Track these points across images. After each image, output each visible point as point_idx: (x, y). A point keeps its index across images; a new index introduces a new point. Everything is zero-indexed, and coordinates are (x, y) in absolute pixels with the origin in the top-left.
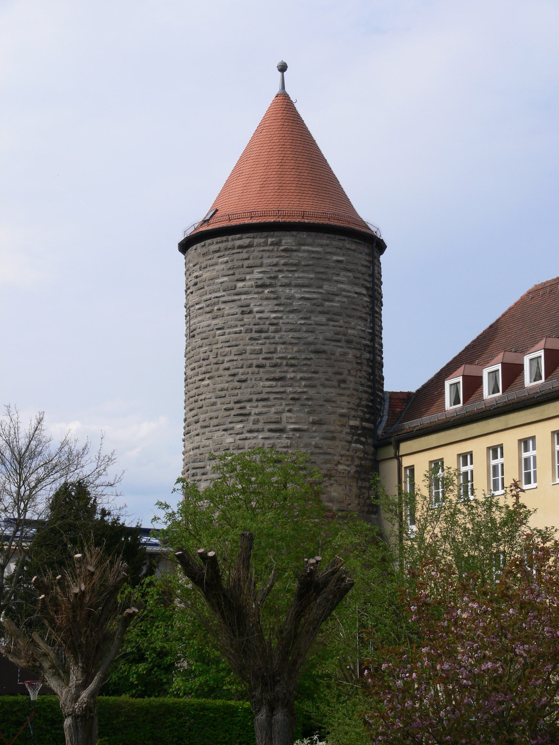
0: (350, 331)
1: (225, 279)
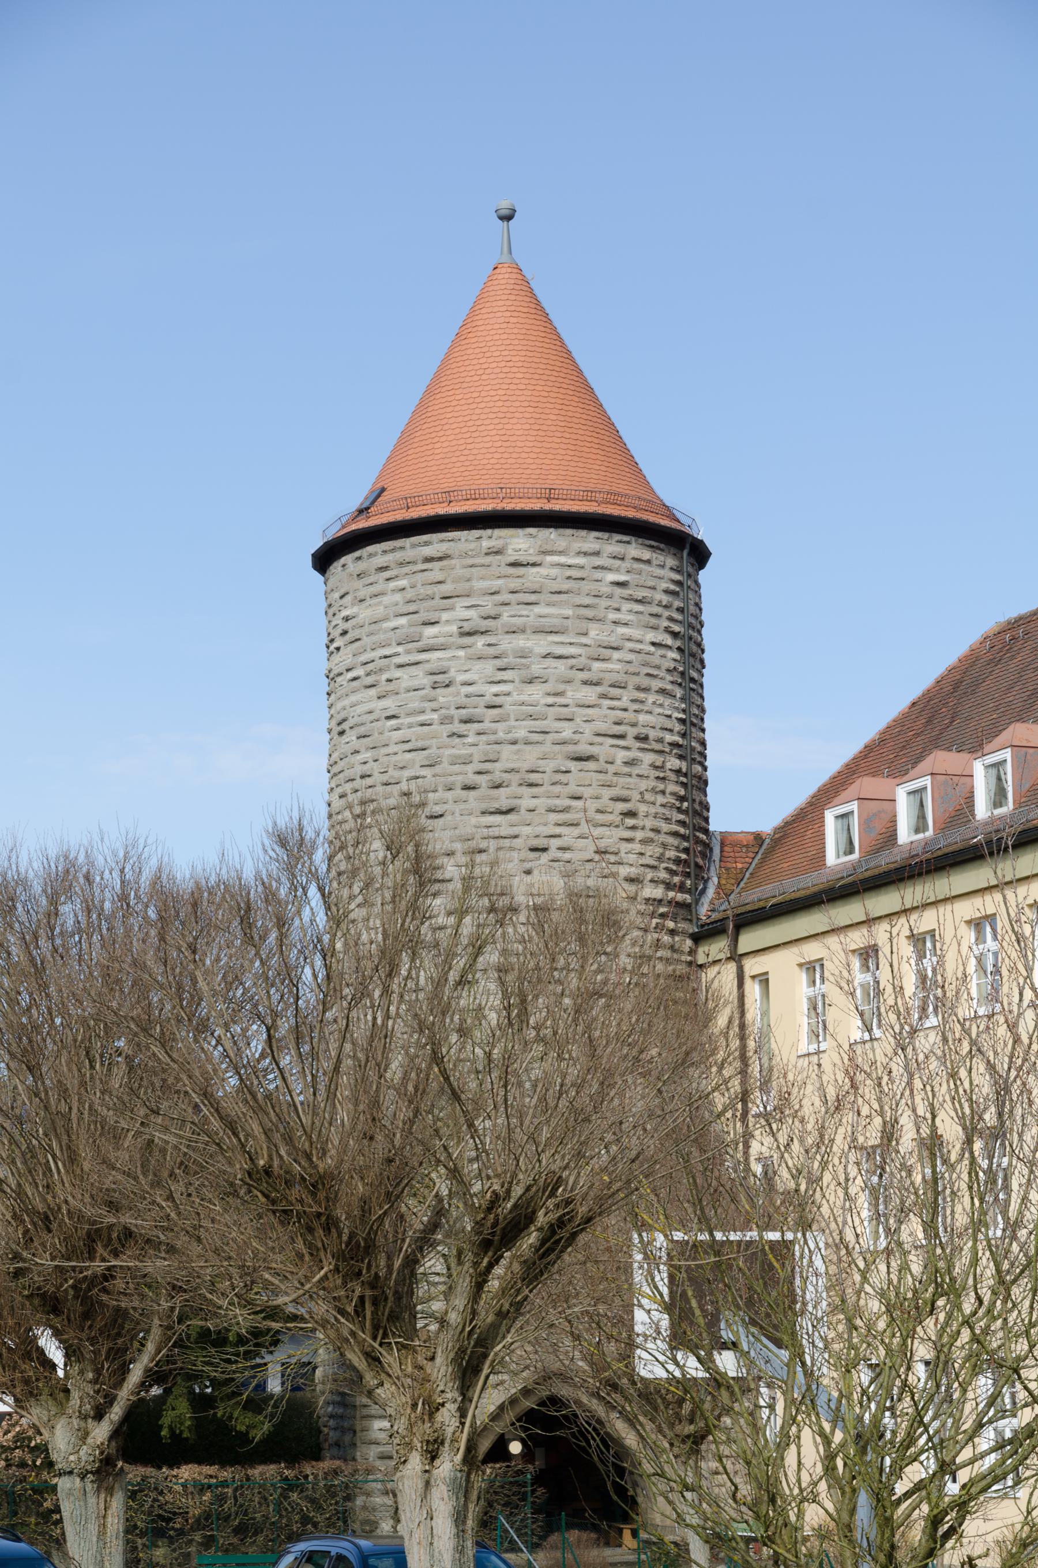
0: (642, 718)
1: (403, 621)
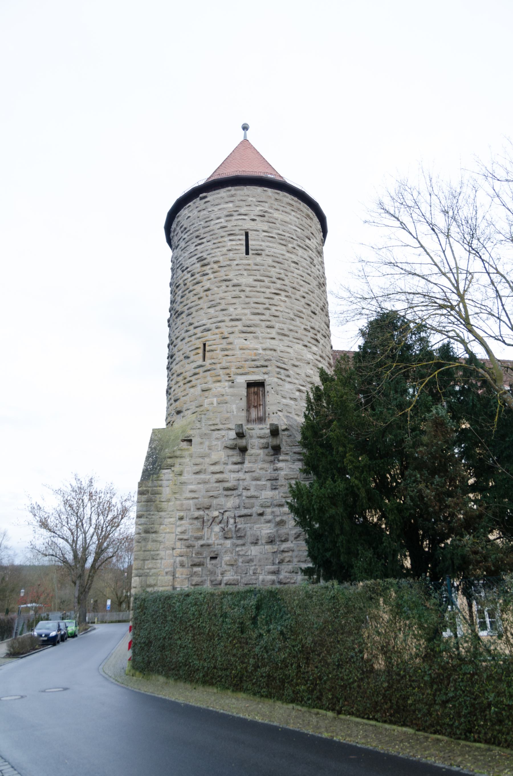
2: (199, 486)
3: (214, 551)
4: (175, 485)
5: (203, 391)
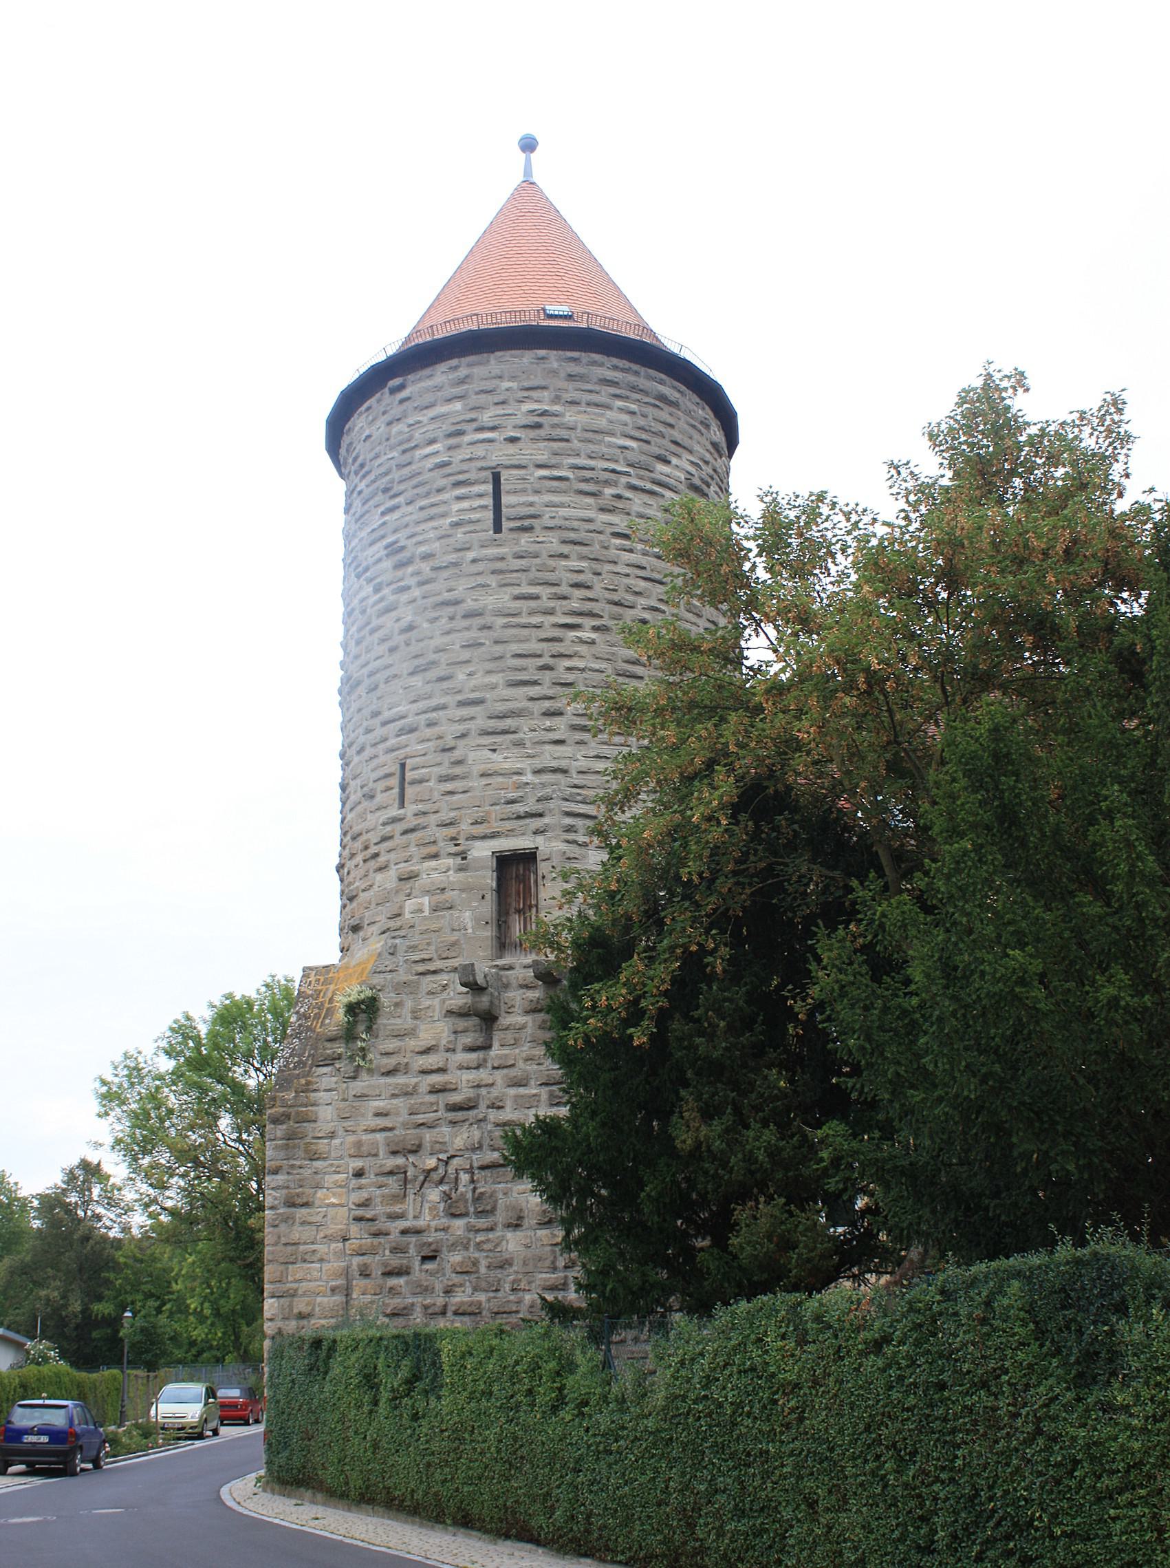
1: (633, 444)
2: (395, 1101)
3: (430, 1244)
4: (344, 1100)
5: (401, 880)
